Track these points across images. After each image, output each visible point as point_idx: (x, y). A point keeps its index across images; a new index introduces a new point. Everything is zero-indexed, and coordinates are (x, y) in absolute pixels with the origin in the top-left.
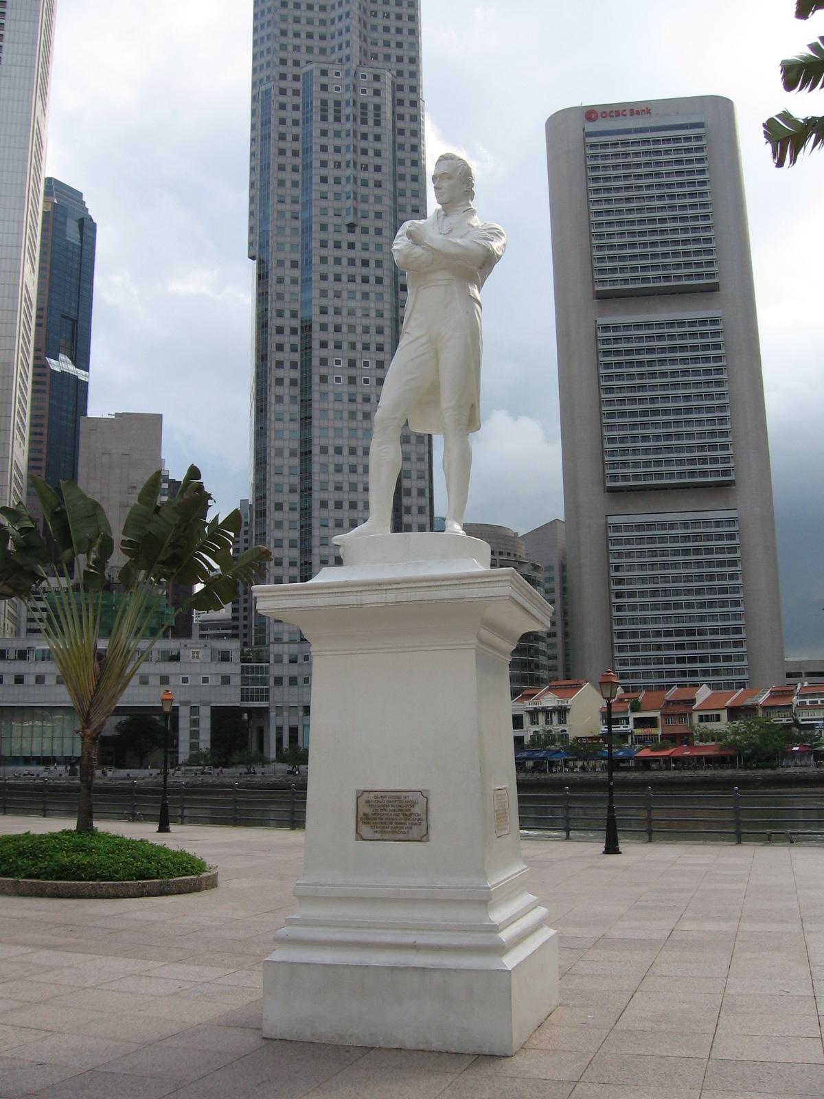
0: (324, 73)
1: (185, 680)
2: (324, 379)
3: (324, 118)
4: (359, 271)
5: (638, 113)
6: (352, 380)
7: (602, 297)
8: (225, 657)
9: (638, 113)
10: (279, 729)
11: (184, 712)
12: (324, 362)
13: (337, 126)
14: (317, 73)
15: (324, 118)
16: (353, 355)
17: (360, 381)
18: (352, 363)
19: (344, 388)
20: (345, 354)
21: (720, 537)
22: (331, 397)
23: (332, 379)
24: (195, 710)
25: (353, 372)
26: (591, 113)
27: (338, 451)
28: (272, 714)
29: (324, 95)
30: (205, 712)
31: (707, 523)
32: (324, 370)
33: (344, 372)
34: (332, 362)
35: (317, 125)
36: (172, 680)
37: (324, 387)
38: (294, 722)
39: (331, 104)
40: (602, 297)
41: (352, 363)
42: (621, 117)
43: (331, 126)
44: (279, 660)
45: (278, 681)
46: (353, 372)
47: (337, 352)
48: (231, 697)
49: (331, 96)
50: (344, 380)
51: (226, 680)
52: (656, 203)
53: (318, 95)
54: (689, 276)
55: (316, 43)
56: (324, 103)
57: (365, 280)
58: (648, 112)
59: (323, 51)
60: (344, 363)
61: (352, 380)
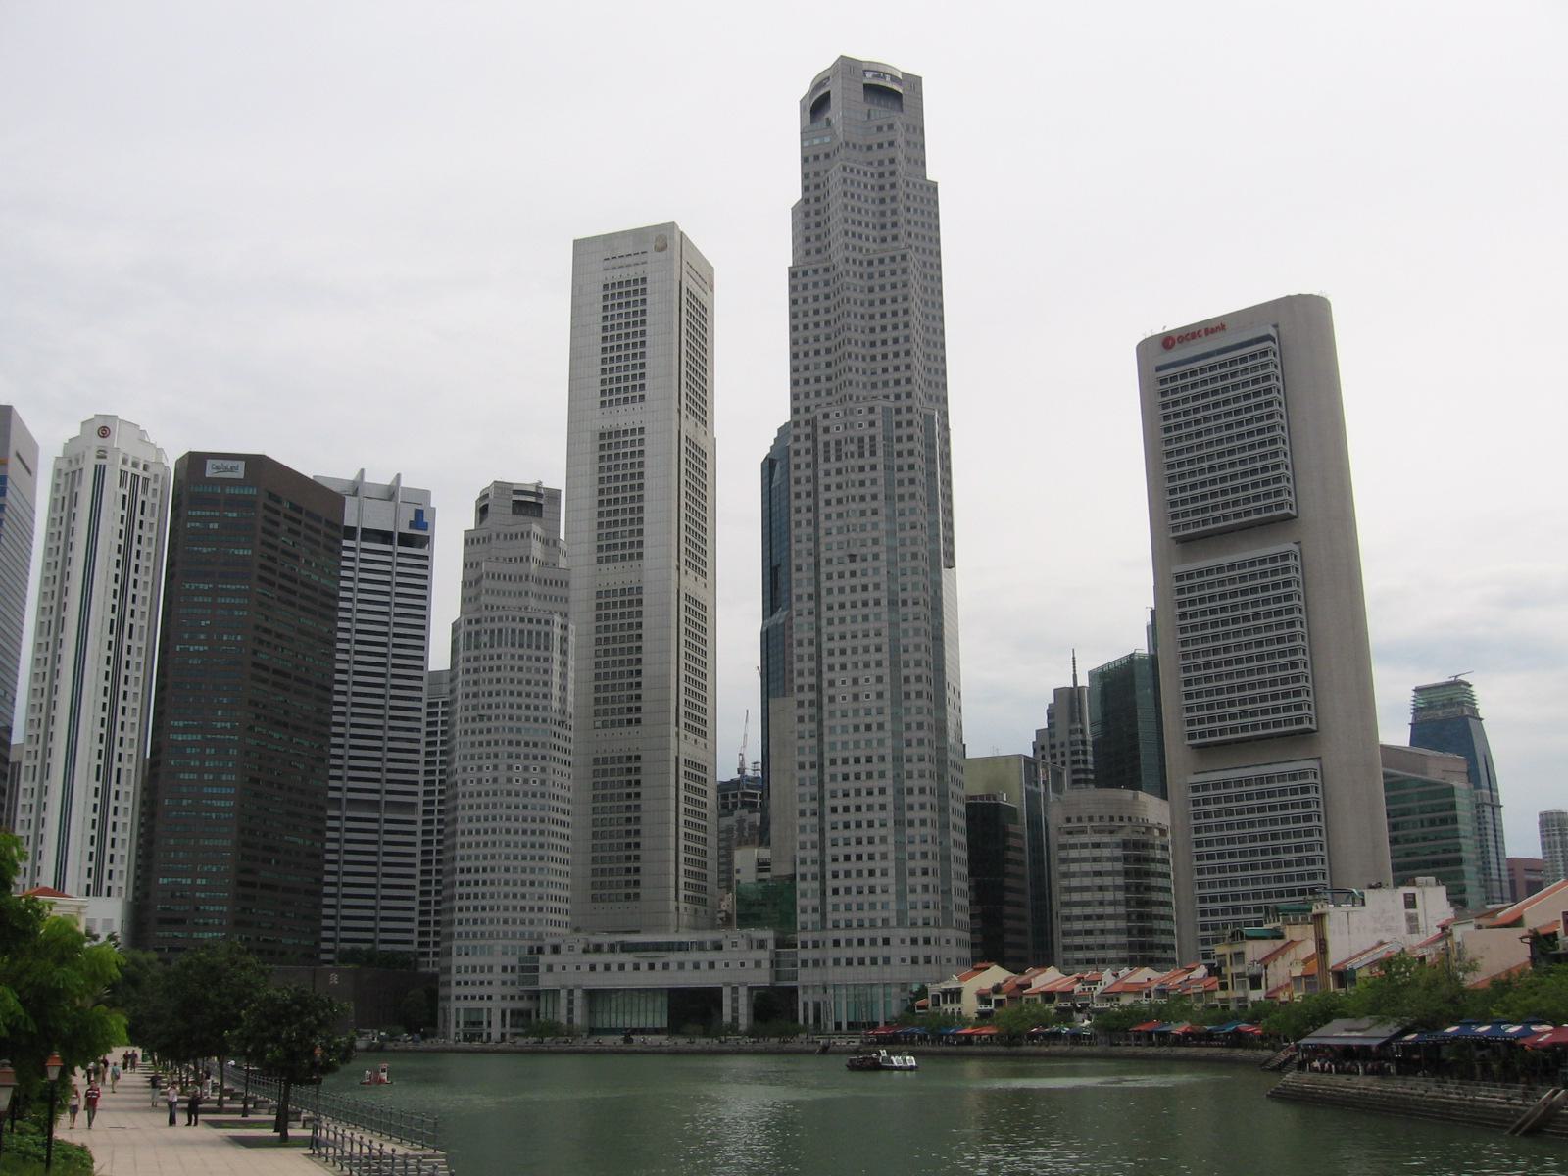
0: (826, 416)
1: (727, 965)
2: (832, 699)
3: (827, 459)
4: (859, 596)
5: (1213, 331)
6: (856, 697)
7: (1184, 541)
8: (762, 944)
9: (1213, 331)
10: (806, 1004)
11: (727, 992)
12: (832, 683)
13: (839, 465)
14: (820, 418)
15: (827, 459)
16: (855, 674)
17: (862, 697)
18: (855, 681)
19: (849, 705)
20: (850, 673)
21: (1294, 791)
22: (838, 714)
23: (839, 699)
24: (735, 990)
25: (856, 689)
26: (1168, 341)
27: (845, 761)
28: (800, 992)
29: (827, 437)
30: (743, 991)
31: (1282, 777)
32: (832, 691)
33: (849, 690)
34: (838, 683)
35: (823, 466)
36: (717, 965)
37: (832, 707)
38: (817, 999)
39: (833, 444)
40: (1184, 541)
41: (855, 681)
42: (1199, 340)
43: (833, 465)
44: (804, 945)
45: (804, 963)
46: (856, 689)
47: (844, 673)
48: (763, 978)
49: (831, 438)
50: (849, 698)
51: (758, 964)
52: (1225, 434)
53: (822, 438)
54: (1258, 511)
55: (824, 385)
56: (827, 444)
57: (865, 604)
58: (1222, 328)
59: (829, 393)
60: (849, 682)
61: (856, 697)
